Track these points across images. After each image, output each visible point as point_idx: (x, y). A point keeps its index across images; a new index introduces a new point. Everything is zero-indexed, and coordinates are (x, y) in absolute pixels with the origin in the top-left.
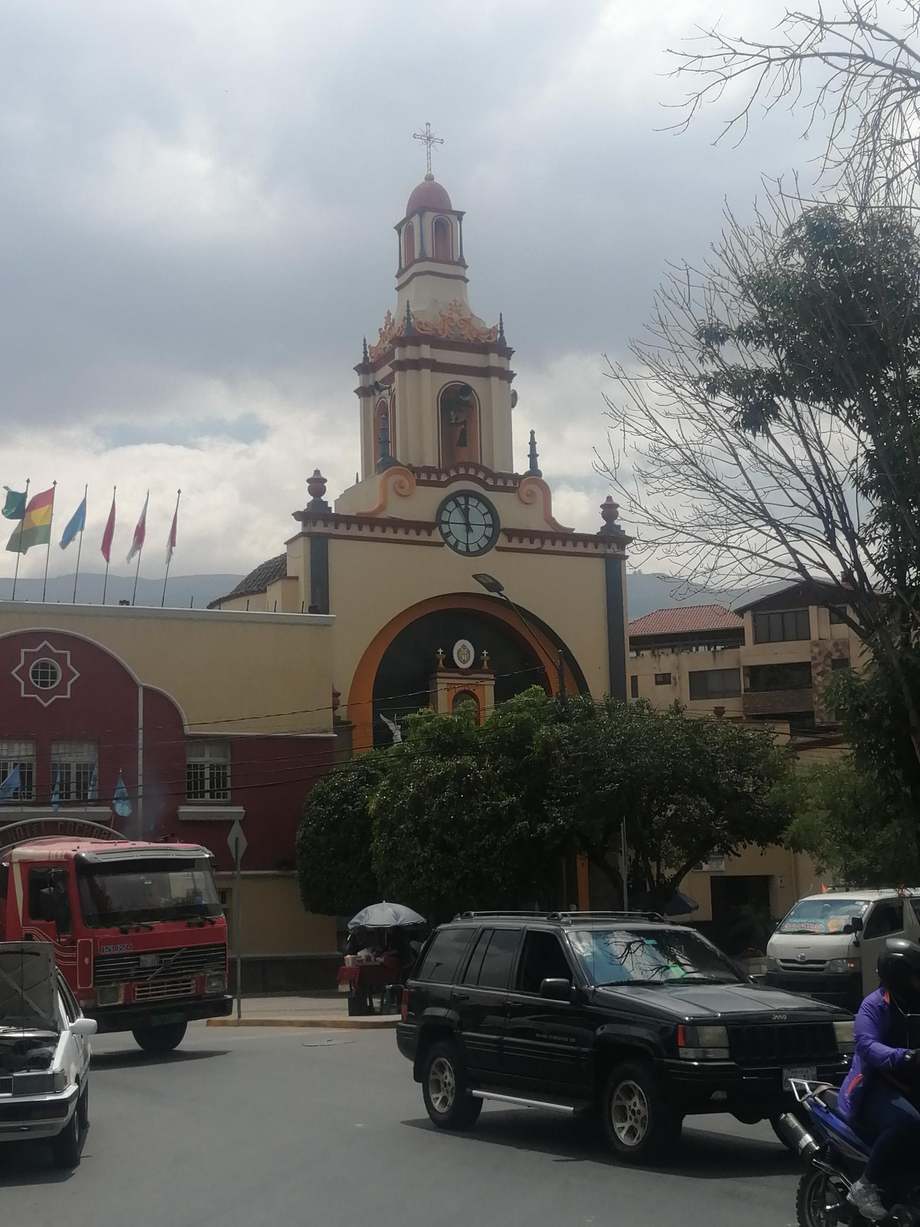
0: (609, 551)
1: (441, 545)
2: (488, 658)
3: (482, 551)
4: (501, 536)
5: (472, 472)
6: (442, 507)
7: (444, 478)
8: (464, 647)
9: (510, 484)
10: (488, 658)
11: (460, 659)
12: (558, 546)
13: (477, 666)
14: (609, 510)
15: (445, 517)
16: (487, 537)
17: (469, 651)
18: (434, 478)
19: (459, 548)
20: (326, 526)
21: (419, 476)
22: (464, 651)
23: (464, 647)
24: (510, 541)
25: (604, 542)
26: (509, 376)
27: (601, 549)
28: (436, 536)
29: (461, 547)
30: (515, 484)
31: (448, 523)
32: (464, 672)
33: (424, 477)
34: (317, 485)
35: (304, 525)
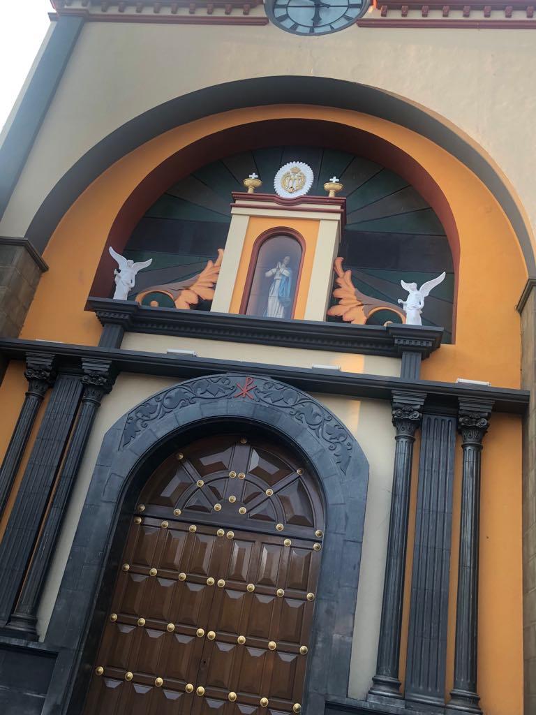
1: (262, 22)
2: (339, 187)
3: (333, 30)
4: (371, 9)
8: (296, 171)
10: (339, 187)
11: (283, 186)
13: (317, 194)
16: (348, 18)
17: (303, 177)
22: (294, 178)
23: (296, 171)
24: (382, 15)
29: (300, 29)
31: (286, 7)
32: (288, 204)
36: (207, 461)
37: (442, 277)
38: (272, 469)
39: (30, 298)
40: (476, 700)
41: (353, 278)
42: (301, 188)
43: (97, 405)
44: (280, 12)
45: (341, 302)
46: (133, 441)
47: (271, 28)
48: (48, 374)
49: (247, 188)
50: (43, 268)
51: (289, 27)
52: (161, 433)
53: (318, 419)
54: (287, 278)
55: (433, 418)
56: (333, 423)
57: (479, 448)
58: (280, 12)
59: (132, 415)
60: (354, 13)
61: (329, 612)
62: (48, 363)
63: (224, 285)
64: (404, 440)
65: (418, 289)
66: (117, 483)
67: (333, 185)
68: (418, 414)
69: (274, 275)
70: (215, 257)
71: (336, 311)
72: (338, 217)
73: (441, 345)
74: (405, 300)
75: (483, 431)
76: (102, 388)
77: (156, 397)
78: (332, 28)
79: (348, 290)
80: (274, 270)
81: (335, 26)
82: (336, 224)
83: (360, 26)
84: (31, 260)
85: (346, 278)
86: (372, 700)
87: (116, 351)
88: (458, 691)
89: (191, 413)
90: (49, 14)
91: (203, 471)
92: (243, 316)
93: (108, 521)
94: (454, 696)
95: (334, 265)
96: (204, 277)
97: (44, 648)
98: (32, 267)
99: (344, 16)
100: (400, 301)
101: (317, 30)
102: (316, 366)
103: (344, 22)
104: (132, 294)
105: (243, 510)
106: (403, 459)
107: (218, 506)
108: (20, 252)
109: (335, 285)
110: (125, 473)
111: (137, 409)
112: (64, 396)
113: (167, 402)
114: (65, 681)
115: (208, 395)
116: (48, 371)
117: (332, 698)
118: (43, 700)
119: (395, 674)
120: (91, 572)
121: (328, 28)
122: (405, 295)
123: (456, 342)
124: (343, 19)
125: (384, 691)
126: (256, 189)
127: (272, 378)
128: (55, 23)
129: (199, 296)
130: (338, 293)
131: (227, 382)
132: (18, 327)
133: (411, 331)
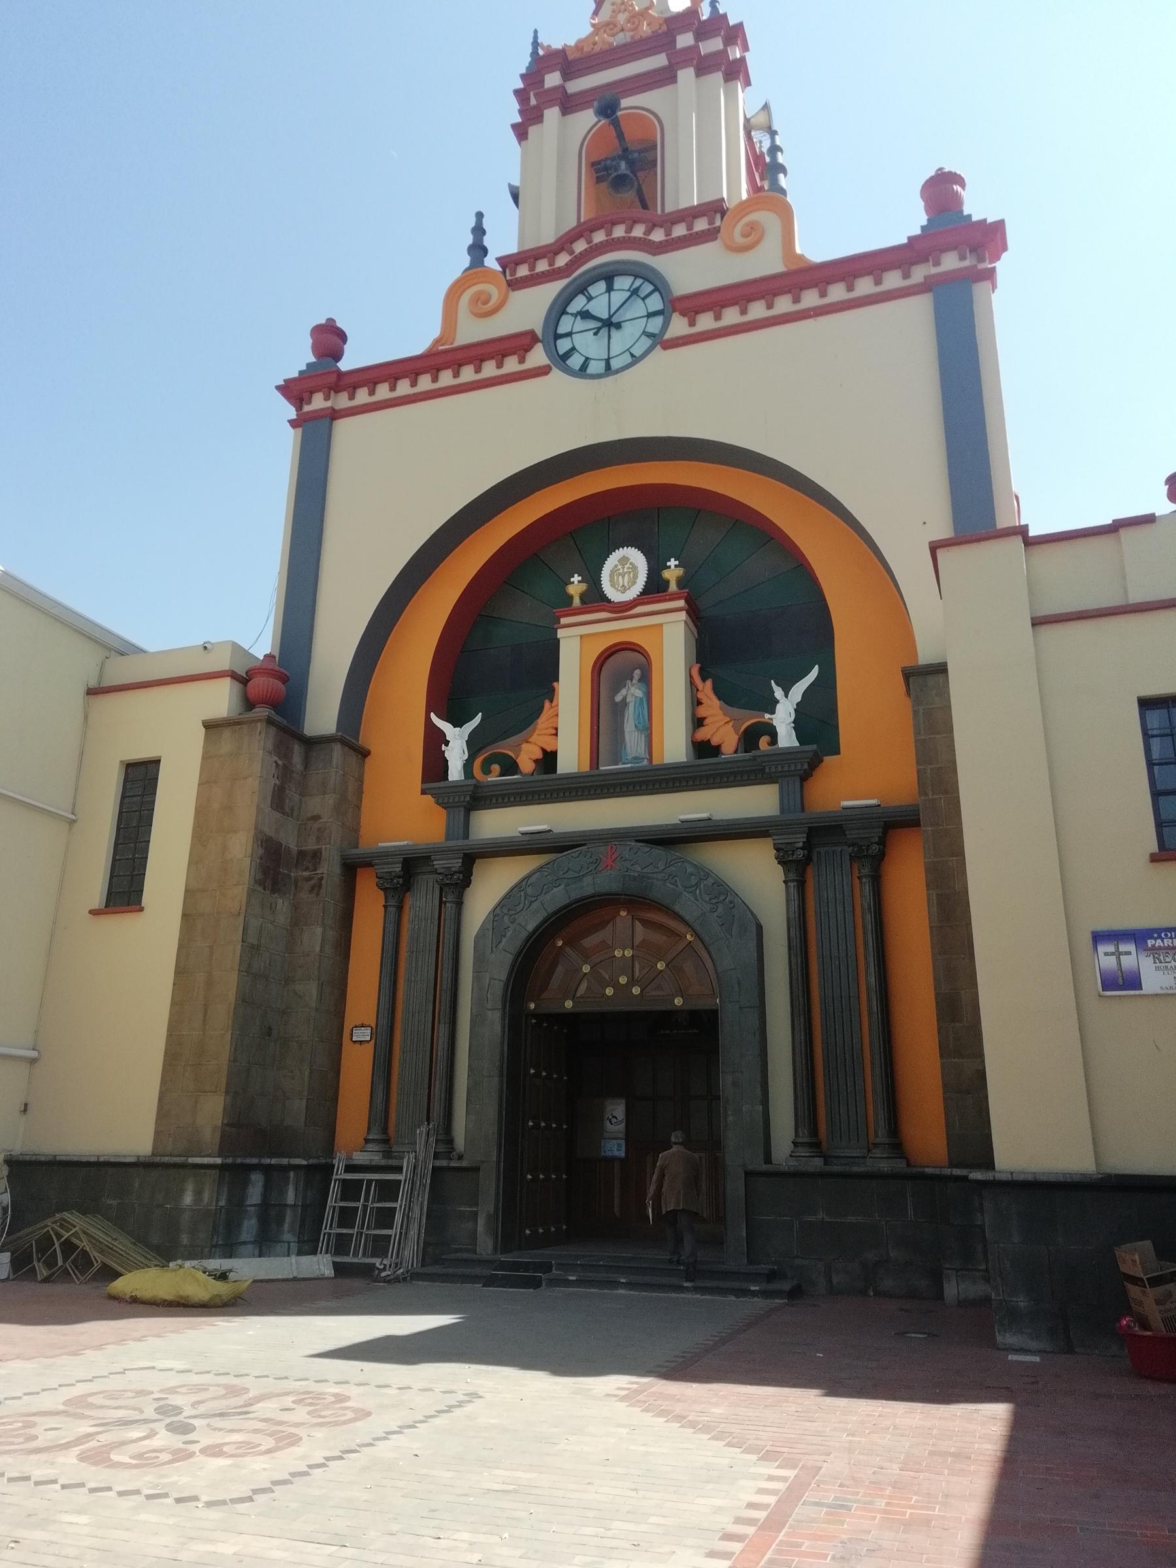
0: (934, 270)
1: (543, 371)
2: (680, 572)
3: (636, 360)
5: (619, 232)
6: (559, 309)
7: (562, 260)
8: (624, 560)
9: (701, 225)
10: (680, 572)
12: (810, 299)
13: (655, 588)
14: (942, 190)
15: (565, 325)
17: (634, 568)
18: (542, 266)
19: (590, 370)
20: (327, 398)
21: (513, 272)
22: (625, 570)
23: (624, 560)
24: (692, 323)
25: (922, 258)
26: (736, 72)
27: (919, 274)
28: (538, 356)
29: (595, 367)
30: (711, 222)
31: (569, 334)
32: (622, 610)
33: (523, 271)
34: (329, 339)
35: (299, 408)
36: (589, 942)
37: (814, 673)
38: (658, 938)
39: (360, 792)
40: (897, 1146)
41: (717, 691)
42: (634, 583)
43: (459, 904)
44: (563, 345)
45: (706, 722)
46: (504, 940)
47: (556, 373)
48: (401, 880)
49: (571, 598)
50: (364, 754)
51: (577, 368)
52: (531, 927)
53: (694, 880)
54: (641, 699)
55: (822, 850)
56: (710, 881)
57: (876, 880)
58: (563, 345)
59: (498, 911)
60: (655, 325)
61: (735, 1084)
62: (398, 868)
63: (566, 729)
64: (792, 884)
65: (786, 696)
66: (498, 989)
67: (673, 571)
68: (800, 854)
69: (625, 698)
70: (551, 694)
71: (703, 734)
72: (683, 615)
73: (825, 758)
74: (773, 712)
75: (881, 857)
76: (459, 883)
77: (518, 886)
78: (632, 356)
79: (712, 706)
80: (624, 692)
81: (637, 354)
82: (681, 628)
83: (665, 348)
84: (351, 752)
85: (706, 689)
86: (793, 1163)
87: (466, 842)
88: (878, 1140)
89: (557, 897)
90: (289, 421)
91: (586, 957)
92: (596, 772)
93: (498, 1028)
94: (876, 1145)
95: (691, 676)
96: (543, 722)
97: (464, 1164)
98: (353, 759)
99: (644, 333)
100: (767, 716)
101: (615, 364)
102: (683, 817)
103: (646, 342)
104: (468, 766)
105: (636, 991)
106: (795, 905)
107: (609, 991)
108: (337, 750)
109: (696, 702)
110: (503, 976)
111: (500, 905)
112: (422, 902)
113: (529, 890)
114: (492, 1191)
115: (571, 874)
116: (399, 877)
117: (750, 1168)
118: (476, 1213)
119: (814, 1132)
120: (492, 1086)
121: (629, 360)
122: (771, 705)
123: (842, 750)
124: (644, 337)
125: (803, 1152)
126: (583, 597)
127: (637, 841)
128: (300, 430)
129: (543, 750)
130: (702, 712)
131: (589, 855)
132: (353, 831)
133: (788, 753)
